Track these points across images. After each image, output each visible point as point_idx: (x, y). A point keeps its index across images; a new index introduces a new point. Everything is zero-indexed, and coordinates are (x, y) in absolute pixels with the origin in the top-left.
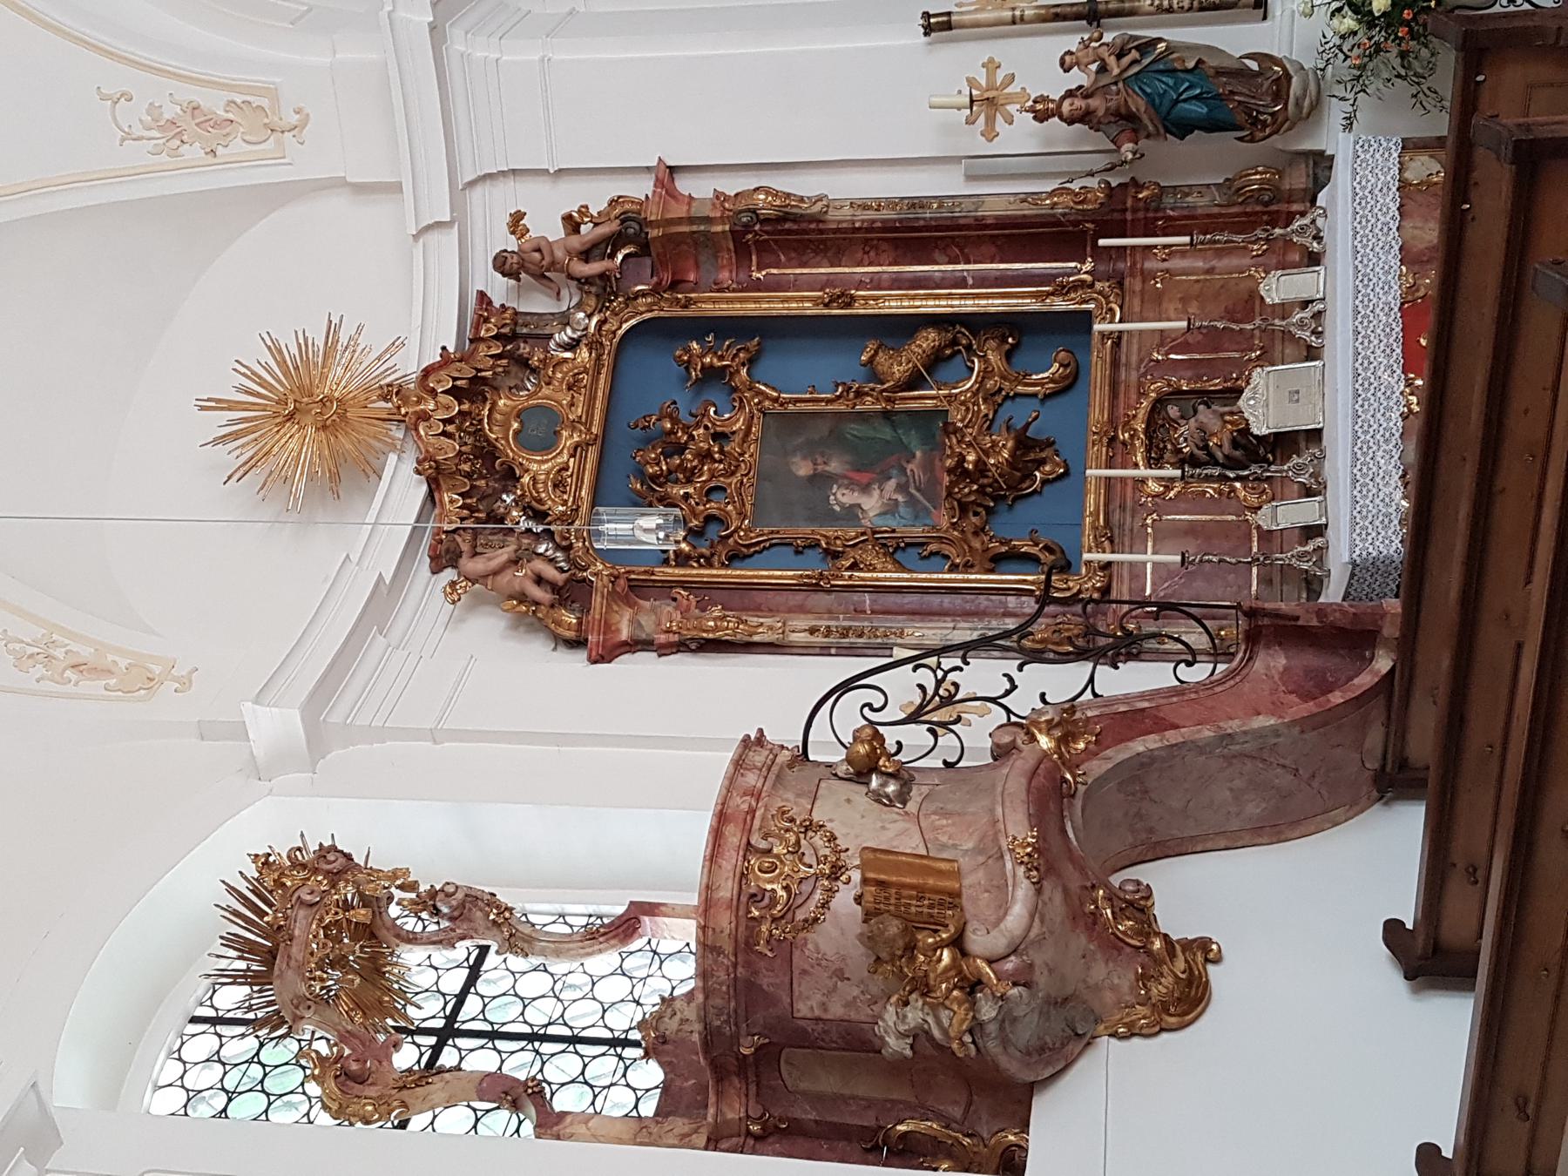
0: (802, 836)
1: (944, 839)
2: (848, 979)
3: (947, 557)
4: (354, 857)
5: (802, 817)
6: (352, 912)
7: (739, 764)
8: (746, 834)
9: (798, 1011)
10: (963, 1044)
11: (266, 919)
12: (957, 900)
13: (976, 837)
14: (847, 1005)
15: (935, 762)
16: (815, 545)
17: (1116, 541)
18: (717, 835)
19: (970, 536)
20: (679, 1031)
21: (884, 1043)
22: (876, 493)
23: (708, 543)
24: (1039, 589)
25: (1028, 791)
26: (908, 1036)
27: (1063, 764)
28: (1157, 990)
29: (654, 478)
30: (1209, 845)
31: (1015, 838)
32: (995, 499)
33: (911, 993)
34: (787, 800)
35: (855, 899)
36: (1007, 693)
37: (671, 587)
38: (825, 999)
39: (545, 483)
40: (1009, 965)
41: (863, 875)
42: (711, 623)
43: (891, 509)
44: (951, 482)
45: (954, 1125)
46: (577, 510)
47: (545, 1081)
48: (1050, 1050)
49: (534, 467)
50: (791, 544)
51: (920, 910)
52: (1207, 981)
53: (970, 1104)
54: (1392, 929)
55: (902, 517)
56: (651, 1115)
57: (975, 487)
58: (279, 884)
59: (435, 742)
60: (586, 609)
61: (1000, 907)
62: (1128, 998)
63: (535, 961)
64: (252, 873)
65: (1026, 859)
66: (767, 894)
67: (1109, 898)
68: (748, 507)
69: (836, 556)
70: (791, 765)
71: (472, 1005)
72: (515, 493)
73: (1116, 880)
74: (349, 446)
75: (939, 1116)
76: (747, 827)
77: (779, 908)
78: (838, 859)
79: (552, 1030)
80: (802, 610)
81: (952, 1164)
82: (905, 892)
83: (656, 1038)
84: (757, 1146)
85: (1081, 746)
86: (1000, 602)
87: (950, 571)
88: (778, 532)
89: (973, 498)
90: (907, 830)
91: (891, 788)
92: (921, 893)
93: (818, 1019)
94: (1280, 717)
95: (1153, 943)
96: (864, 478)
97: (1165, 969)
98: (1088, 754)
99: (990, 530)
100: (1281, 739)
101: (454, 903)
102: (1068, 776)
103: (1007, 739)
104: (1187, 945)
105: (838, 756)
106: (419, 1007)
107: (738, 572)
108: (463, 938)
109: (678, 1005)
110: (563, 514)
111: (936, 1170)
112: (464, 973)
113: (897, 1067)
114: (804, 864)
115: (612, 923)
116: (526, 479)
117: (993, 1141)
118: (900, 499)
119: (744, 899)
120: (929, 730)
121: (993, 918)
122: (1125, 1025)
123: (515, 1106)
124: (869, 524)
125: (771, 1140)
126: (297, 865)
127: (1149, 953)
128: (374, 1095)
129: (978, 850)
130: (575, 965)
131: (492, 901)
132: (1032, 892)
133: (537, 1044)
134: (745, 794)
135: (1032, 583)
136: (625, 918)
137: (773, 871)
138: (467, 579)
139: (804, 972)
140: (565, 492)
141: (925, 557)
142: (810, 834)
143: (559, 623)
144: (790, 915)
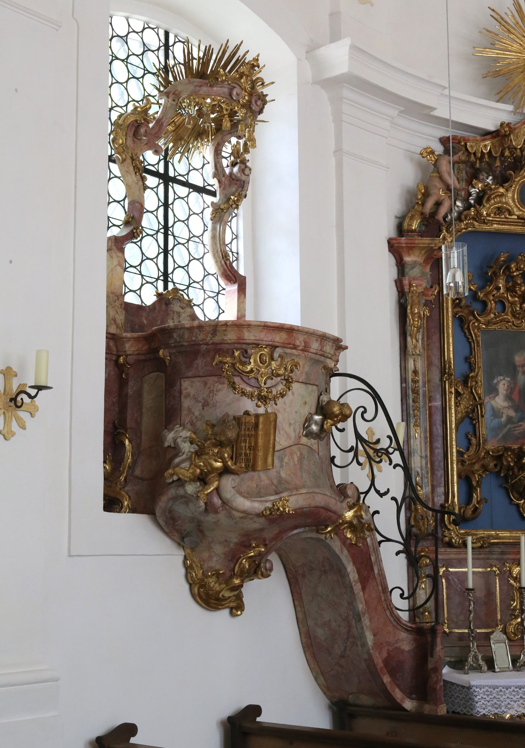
0: (283, 377)
1: (286, 460)
2: (203, 409)
3: (468, 449)
4: (261, 115)
5: (294, 377)
6: (228, 119)
7: (323, 337)
8: (282, 345)
9: (185, 381)
10: (172, 475)
11: (222, 70)
12: (251, 469)
14: (189, 410)
15: (335, 451)
16: (472, 369)
17: (481, 550)
18: (280, 328)
19: (482, 462)
21: (170, 430)
22: (506, 404)
23: (469, 304)
24: (449, 505)
25: (317, 507)
26: (175, 444)
27: (337, 526)
28: (212, 582)
29: (508, 268)
31: (287, 501)
32: (506, 477)
33: (197, 445)
34: (304, 367)
35: (247, 411)
36: (378, 492)
37: (439, 285)
38: (192, 396)
39: (500, 202)
40: (216, 500)
41: (261, 415)
42: (416, 311)
43: (496, 413)
44: (514, 449)
45: (130, 471)
46: (484, 223)
47: (142, 238)
48: (174, 523)
49: (510, 195)
50: (471, 354)
51: (244, 448)
52: (219, 609)
53: (142, 479)
54: (255, 710)
55: (492, 421)
56: (125, 300)
57: (512, 464)
58: (242, 75)
59: (335, 152)
60: (422, 234)
61: (248, 494)
62: (206, 565)
63: (209, 224)
64: (249, 58)
65: (276, 507)
66: (247, 360)
67: (260, 554)
68: (493, 327)
69: (465, 381)
70: (325, 368)
71: (182, 191)
72: (492, 184)
73: (273, 557)
74: (517, 81)
75: (135, 462)
76: (286, 345)
77: (241, 367)
78: (270, 399)
79: (171, 238)
80: (430, 364)
81: (109, 471)
82: (253, 439)
84: (112, 362)
85: (349, 536)
86: (440, 483)
87: (458, 452)
88: (478, 346)
89: (505, 463)
91: (314, 428)
92: (254, 448)
93: (180, 392)
95: (237, 579)
96: (516, 396)
97: (223, 586)
98: (344, 540)
99: (486, 475)
100: (360, 648)
102: (329, 529)
103: (350, 492)
104: (239, 598)
105: (334, 395)
106: (179, 161)
107: (450, 324)
108: (219, 182)
109: (188, 310)
110: (482, 215)
111: (105, 462)
112: (200, 184)
113: (159, 438)
114: (266, 380)
115: (232, 267)
116: (501, 190)
117: (124, 493)
118: (504, 419)
119: (244, 346)
120: (352, 447)
121: (242, 490)
122: (191, 565)
123: (127, 223)
124: (486, 401)
125: (116, 369)
126: (254, 83)
127: (231, 577)
128: (128, 143)
129: (280, 480)
130: (208, 247)
131: (241, 196)
132: (257, 511)
133: (162, 231)
134: (305, 342)
135: (453, 501)
136: (236, 275)
137: (261, 362)
138: (436, 161)
139: (206, 384)
140: (495, 214)
141: (467, 436)
142: (284, 382)
143: (412, 218)
144: (236, 373)
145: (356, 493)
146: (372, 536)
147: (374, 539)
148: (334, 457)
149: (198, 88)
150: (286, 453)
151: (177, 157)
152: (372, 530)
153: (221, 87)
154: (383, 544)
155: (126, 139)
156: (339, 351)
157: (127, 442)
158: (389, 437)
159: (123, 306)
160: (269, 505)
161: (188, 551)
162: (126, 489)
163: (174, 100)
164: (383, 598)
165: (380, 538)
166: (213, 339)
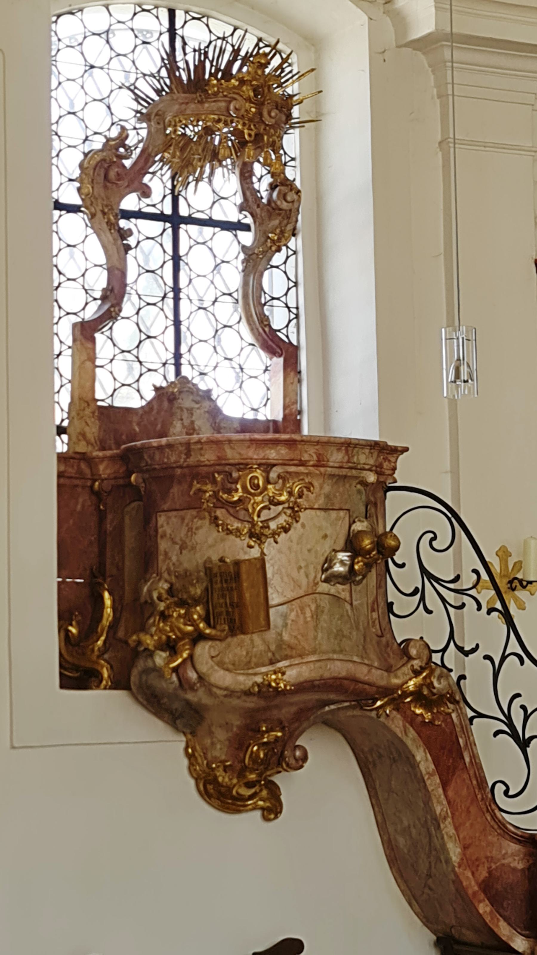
13: (293, 641)
14: (166, 553)
15: (392, 595)
20: (181, 409)
30: (376, 809)
34: (321, 488)
36: (460, 649)
38: (168, 536)
40: (192, 675)
61: (234, 664)
77: (225, 496)
83: (173, 393)
90: (299, 586)
93: (156, 531)
94: (460, 866)
95: (251, 773)
101: (279, 203)
102: (379, 703)
103: (413, 652)
113: (137, 591)
117: (103, 662)
119: (227, 468)
129: (281, 644)
134: (319, 455)
139: (183, 519)
142: (289, 512)
144: (220, 504)
145: (426, 652)
146: (459, 711)
147: (461, 715)
148: (392, 603)
149: (184, 106)
150: (294, 607)
151: (192, 186)
152: (458, 702)
153: (214, 101)
154: (475, 721)
155: (93, 188)
156: (395, 455)
157: (106, 595)
158: (475, 571)
159: (96, 414)
160: (259, 679)
161: (189, 736)
162: (106, 656)
163: (158, 123)
164: (479, 796)
165: (470, 714)
166: (188, 460)
